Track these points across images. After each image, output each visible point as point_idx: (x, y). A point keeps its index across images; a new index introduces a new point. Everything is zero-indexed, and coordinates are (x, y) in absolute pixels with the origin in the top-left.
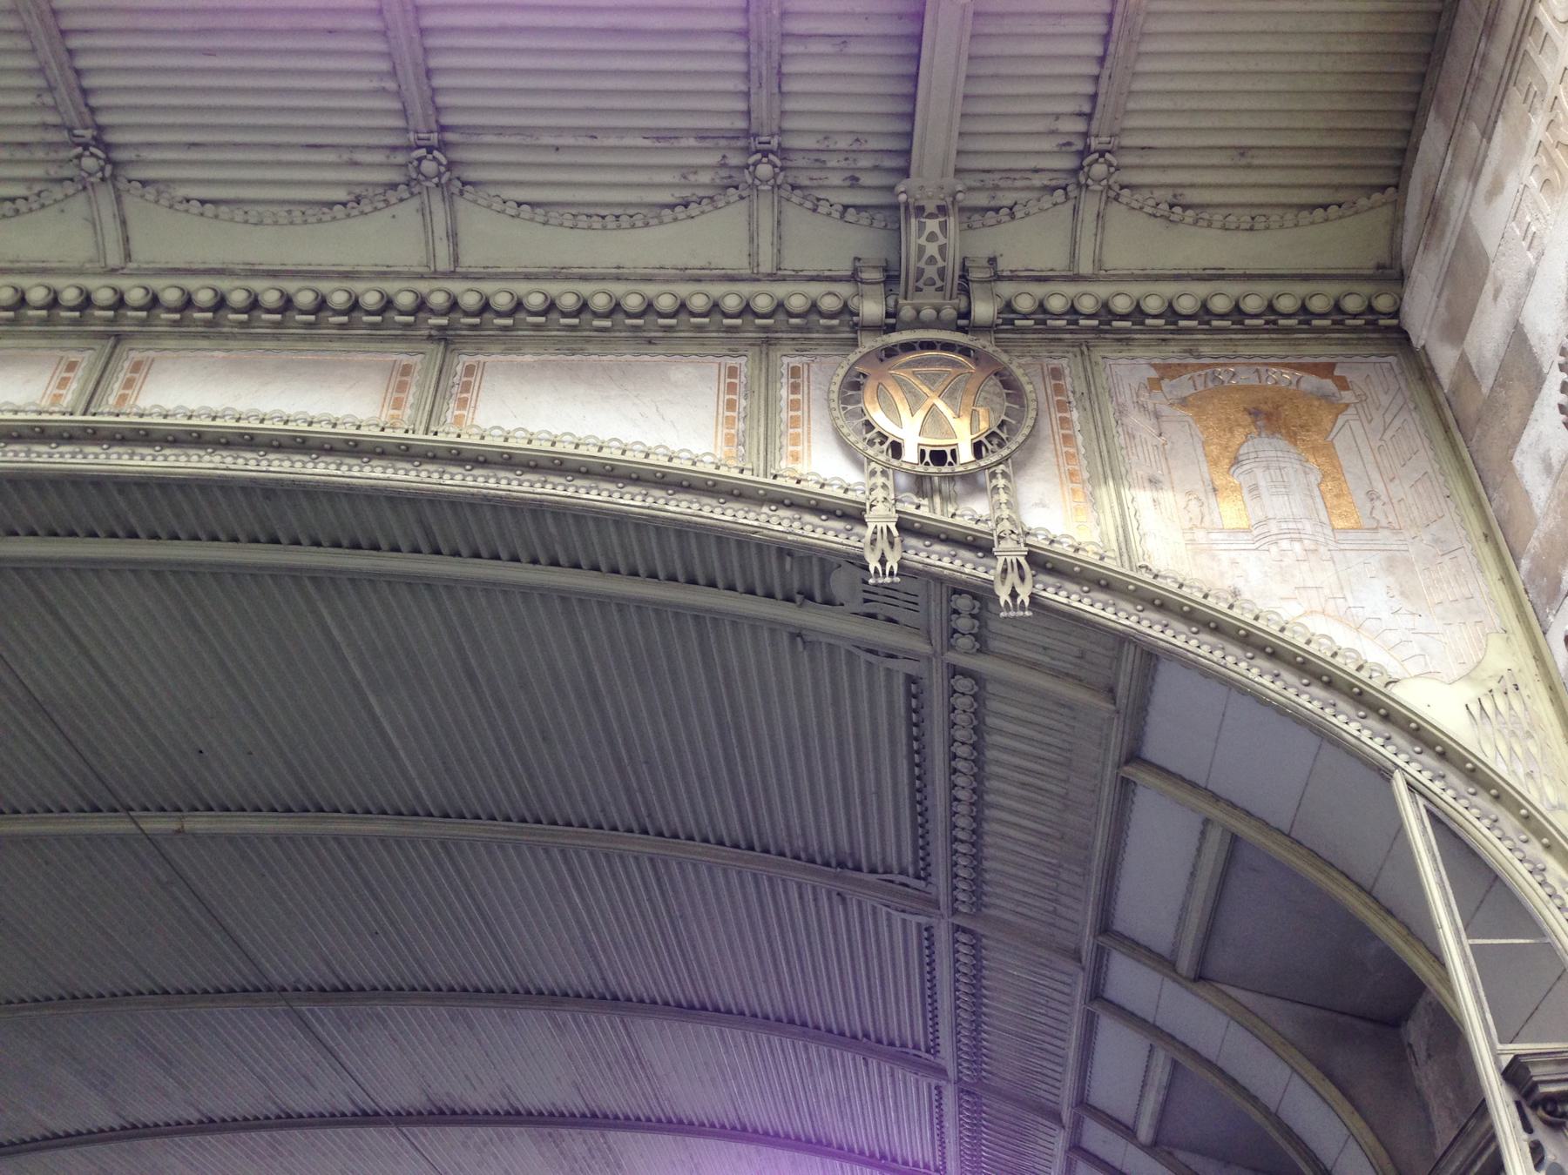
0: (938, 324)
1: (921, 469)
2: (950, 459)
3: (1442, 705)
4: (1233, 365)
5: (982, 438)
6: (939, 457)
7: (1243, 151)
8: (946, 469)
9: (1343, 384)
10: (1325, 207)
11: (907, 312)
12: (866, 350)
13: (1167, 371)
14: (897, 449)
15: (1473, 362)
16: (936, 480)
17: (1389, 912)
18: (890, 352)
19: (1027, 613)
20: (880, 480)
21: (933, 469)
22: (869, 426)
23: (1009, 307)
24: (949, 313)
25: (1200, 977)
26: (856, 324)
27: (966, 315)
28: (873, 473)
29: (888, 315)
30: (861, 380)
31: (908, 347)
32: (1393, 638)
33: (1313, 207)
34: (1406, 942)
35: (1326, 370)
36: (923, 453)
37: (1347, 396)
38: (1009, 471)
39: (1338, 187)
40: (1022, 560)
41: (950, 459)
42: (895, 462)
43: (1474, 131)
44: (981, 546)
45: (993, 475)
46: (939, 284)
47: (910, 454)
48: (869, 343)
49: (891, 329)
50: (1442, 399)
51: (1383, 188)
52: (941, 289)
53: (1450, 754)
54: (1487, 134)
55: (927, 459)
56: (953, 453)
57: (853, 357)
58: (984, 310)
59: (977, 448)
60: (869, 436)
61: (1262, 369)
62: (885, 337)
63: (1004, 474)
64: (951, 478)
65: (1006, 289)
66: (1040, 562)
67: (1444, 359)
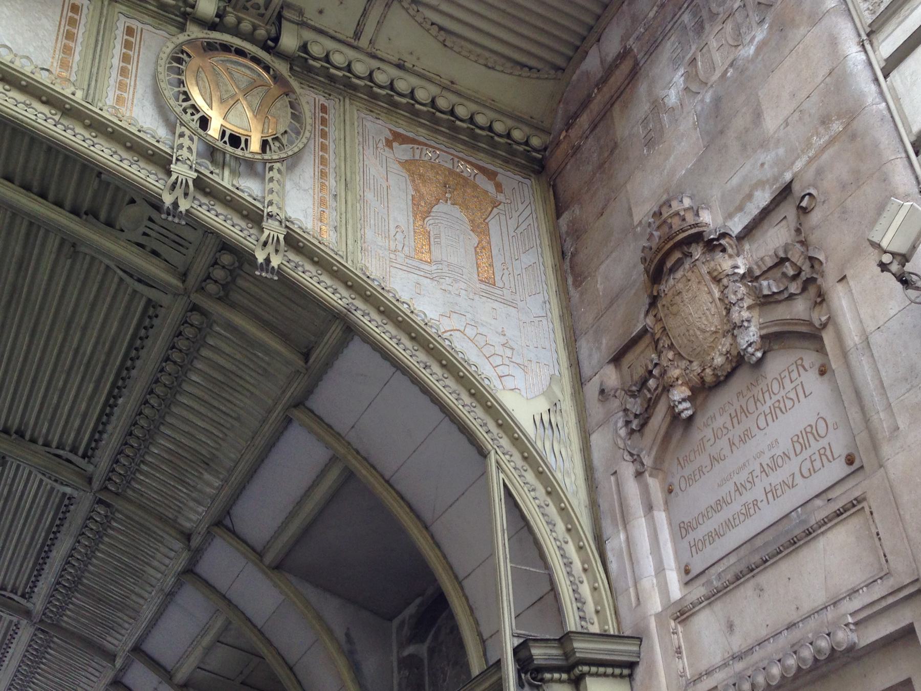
0: (250, 37)
1: (220, 144)
2: (243, 145)
4: (438, 149)
5: (269, 139)
6: (235, 140)
8: (238, 152)
9: (499, 187)
11: (230, 19)
12: (193, 36)
13: (398, 138)
14: (204, 122)
16: (228, 156)
18: (210, 47)
19: (276, 278)
20: (186, 142)
21: (229, 148)
22: (187, 98)
23: (304, 48)
24: (261, 33)
25: (278, 567)
26: (189, 14)
27: (276, 40)
28: (182, 135)
29: (218, 15)
30: (184, 57)
31: (226, 48)
32: (498, 361)
36: (223, 133)
37: (500, 197)
38: (283, 169)
40: (281, 237)
41: (243, 145)
42: (200, 131)
44: (254, 217)
45: (271, 169)
46: (262, 11)
47: (214, 131)
48: (195, 32)
49: (213, 27)
52: (262, 15)
55: (226, 138)
56: (246, 141)
57: (182, 38)
58: (289, 41)
59: (265, 144)
60: (185, 104)
61: (456, 160)
62: (209, 32)
63: (279, 171)
64: (237, 159)
65: (308, 35)
66: (293, 242)
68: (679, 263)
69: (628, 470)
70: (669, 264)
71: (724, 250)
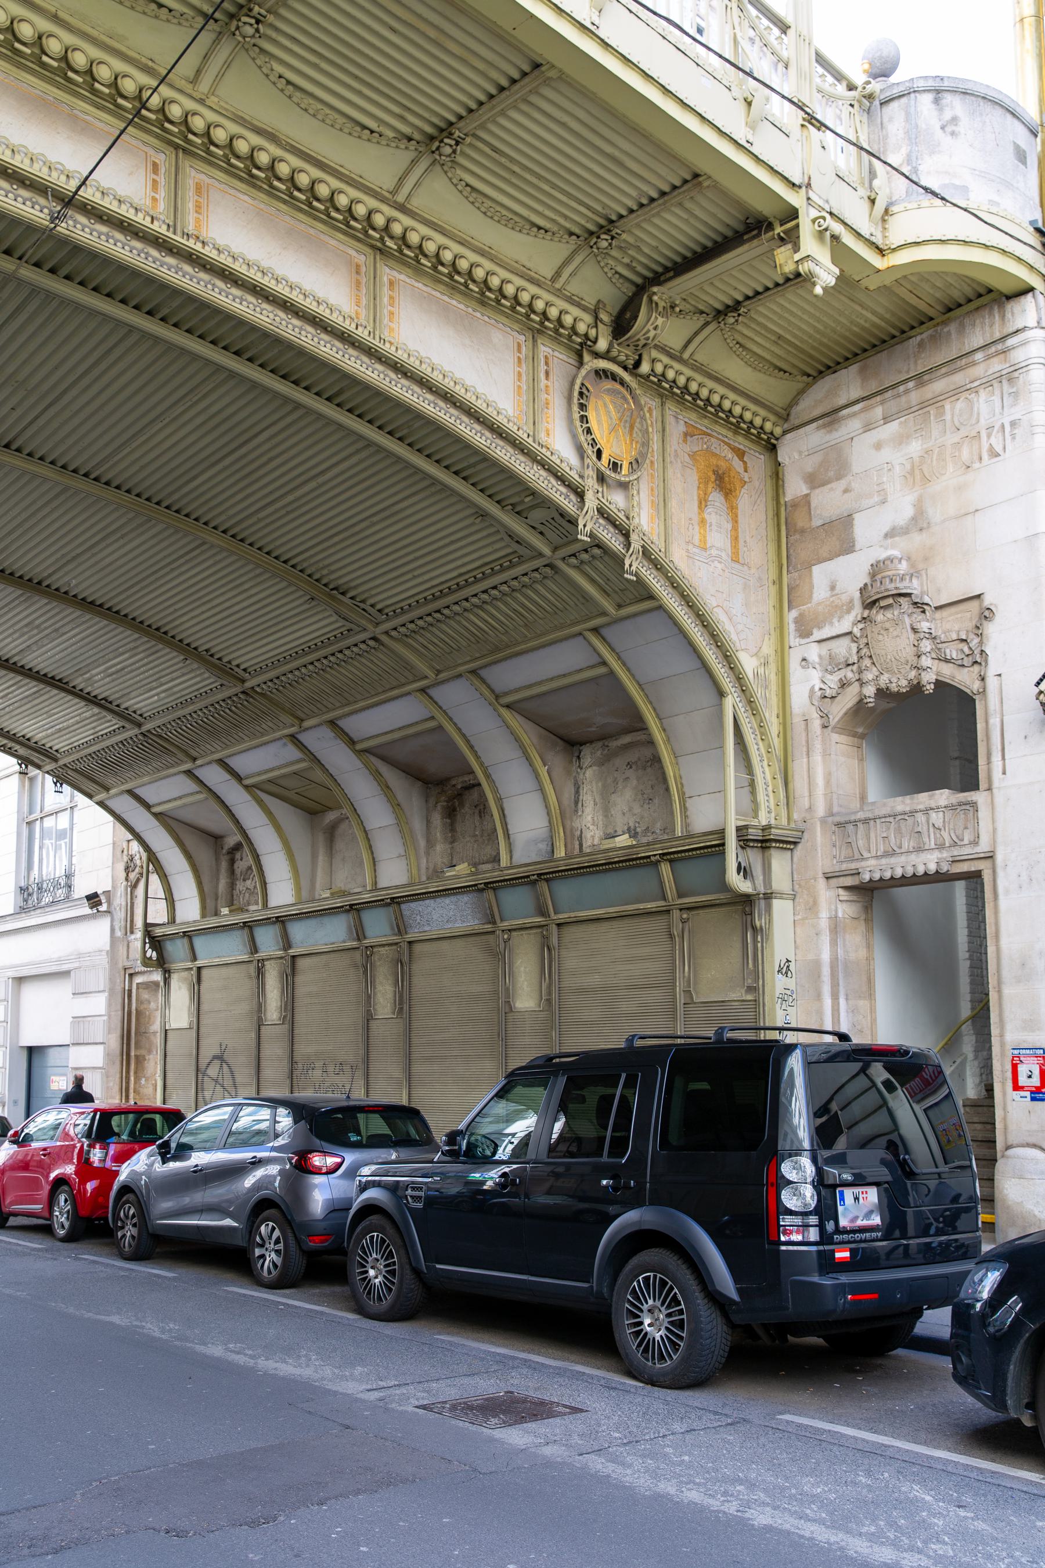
3: (748, 664)
7: (780, 337)
10: (785, 372)
15: (813, 505)
17: (664, 730)
32: (740, 627)
33: (780, 370)
34: (664, 743)
35: (741, 454)
39: (794, 366)
43: (879, 412)
50: (782, 502)
51: (809, 375)
53: (747, 693)
54: (887, 419)
67: (795, 487)
68: (888, 607)
69: (816, 723)
70: (883, 603)
71: (924, 612)
